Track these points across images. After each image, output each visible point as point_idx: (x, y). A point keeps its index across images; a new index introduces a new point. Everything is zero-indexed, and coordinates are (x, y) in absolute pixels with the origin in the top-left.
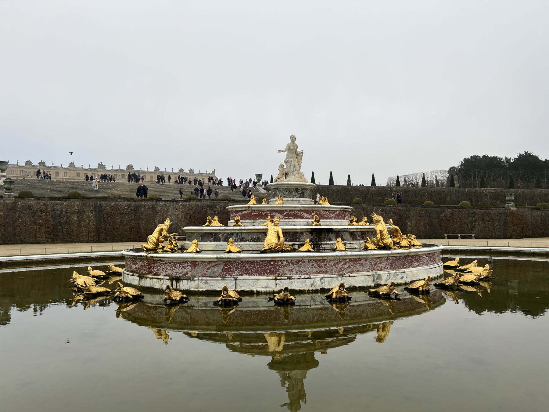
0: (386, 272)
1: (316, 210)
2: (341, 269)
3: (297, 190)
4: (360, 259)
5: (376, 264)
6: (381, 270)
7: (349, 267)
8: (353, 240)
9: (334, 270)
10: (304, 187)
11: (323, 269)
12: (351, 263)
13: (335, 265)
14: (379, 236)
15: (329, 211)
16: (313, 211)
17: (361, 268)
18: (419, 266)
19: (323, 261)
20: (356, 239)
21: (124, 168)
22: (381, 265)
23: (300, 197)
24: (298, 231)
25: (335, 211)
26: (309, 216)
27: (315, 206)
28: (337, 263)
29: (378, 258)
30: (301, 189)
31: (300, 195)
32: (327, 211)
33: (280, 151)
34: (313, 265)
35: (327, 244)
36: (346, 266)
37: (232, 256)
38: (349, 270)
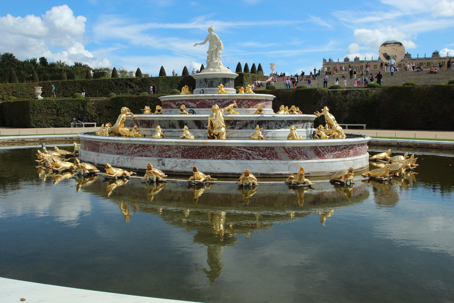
0: (173, 160)
1: (200, 100)
2: (132, 152)
3: (206, 80)
4: (147, 146)
5: (164, 151)
6: (170, 157)
7: (139, 151)
8: (199, 128)
9: (127, 153)
10: (210, 77)
11: (121, 151)
12: (140, 148)
13: (128, 148)
14: (209, 125)
15: (215, 100)
16: (198, 100)
17: (149, 154)
18: (227, 158)
19: (121, 144)
20: (203, 128)
21: (429, 55)
22: (169, 153)
23: (209, 87)
24: (150, 119)
25: (224, 100)
26: (194, 106)
27: (237, 94)
28: (130, 147)
29: (167, 146)
30: (210, 79)
31: (209, 84)
32: (213, 100)
33: (196, 44)
34: (115, 147)
35: (170, 131)
36: (136, 151)
38: (139, 154)
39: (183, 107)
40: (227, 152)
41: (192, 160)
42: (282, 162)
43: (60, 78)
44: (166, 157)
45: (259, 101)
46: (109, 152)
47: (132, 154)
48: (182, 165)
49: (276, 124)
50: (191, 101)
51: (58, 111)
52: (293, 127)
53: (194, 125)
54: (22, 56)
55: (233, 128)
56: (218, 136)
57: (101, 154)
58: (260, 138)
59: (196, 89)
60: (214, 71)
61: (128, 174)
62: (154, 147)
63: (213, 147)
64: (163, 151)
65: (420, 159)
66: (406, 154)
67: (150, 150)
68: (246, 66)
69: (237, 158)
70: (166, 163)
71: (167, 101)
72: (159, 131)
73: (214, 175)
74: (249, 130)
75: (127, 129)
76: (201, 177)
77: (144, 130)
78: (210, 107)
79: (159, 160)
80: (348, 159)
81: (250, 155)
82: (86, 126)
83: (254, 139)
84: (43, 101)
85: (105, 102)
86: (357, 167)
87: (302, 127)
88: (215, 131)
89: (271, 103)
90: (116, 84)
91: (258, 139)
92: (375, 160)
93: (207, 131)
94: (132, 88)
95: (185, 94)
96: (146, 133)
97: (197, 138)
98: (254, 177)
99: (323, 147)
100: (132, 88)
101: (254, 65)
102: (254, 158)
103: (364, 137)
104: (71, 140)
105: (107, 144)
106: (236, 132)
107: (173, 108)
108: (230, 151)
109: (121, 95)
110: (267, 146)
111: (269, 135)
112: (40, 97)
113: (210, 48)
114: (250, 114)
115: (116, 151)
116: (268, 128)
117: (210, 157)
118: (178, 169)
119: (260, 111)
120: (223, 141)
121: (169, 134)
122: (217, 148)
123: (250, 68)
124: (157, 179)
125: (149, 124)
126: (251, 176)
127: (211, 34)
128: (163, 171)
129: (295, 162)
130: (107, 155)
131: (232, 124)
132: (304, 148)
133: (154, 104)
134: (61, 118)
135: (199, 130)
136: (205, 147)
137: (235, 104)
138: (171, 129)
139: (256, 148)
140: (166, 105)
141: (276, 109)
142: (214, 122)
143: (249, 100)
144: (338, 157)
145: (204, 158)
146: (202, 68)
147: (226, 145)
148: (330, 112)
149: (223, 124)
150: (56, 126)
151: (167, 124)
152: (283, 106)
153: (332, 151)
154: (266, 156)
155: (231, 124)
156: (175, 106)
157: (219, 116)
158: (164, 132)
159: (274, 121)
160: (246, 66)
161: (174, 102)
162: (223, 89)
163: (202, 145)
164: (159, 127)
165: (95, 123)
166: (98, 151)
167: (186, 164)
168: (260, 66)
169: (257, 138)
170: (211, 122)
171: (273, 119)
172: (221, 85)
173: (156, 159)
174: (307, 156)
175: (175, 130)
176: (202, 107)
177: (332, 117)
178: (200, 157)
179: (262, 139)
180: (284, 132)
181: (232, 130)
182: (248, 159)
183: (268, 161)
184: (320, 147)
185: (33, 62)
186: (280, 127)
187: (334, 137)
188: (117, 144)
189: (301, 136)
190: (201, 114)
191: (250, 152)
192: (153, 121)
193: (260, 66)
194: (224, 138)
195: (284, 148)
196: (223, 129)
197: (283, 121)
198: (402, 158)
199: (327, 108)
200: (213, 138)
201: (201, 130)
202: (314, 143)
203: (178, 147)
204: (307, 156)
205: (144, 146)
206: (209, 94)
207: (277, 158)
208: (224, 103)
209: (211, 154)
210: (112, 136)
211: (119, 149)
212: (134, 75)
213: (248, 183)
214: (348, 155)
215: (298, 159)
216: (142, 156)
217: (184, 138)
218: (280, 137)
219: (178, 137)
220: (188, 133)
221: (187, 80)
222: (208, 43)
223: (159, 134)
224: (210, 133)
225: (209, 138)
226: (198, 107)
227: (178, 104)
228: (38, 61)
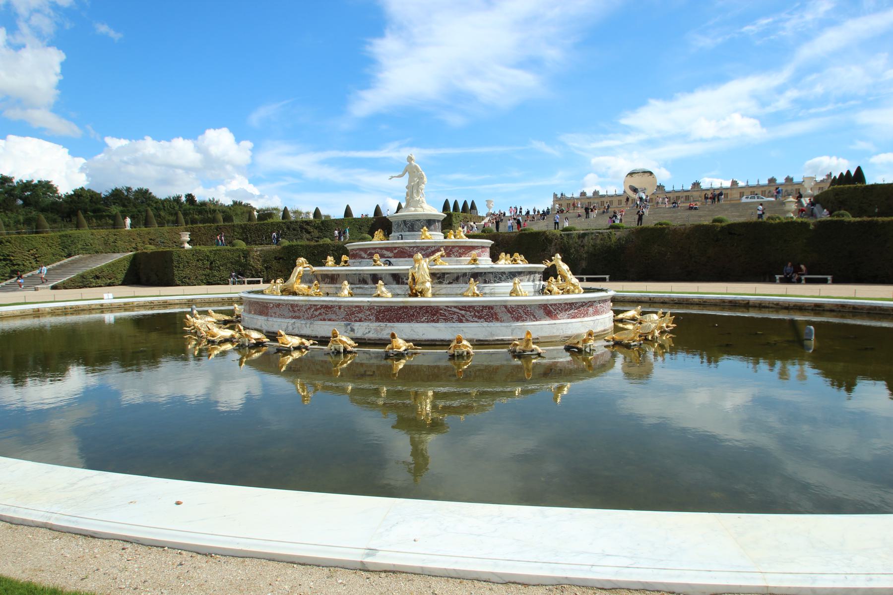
0: (365, 324)
3: (405, 221)
4: (332, 307)
6: (360, 321)
7: (320, 314)
8: (398, 283)
11: (297, 314)
12: (323, 310)
16: (395, 248)
18: (433, 321)
19: (297, 306)
20: (403, 283)
22: (360, 315)
26: (391, 255)
29: (357, 306)
37: (311, 298)
38: (320, 317)
39: (376, 257)
40: (433, 314)
41: (389, 324)
42: (503, 324)
43: (214, 220)
44: (356, 321)
45: (473, 248)
46: (282, 316)
47: (312, 317)
48: (376, 330)
49: (496, 277)
50: (387, 249)
51: (211, 263)
52: (517, 280)
53: (391, 279)
54: (161, 193)
55: (440, 283)
56: (422, 293)
57: (270, 319)
58: (475, 295)
59: (393, 234)
60: (415, 211)
61: (307, 343)
62: (340, 308)
63: (416, 307)
64: (352, 314)
65: (677, 318)
66: (661, 311)
67: (335, 313)
68: (456, 203)
69: (446, 320)
70: (355, 328)
71: (355, 250)
72: (346, 288)
73: (418, 343)
74: (461, 285)
75: (304, 286)
76: (401, 345)
77: (326, 287)
78: (411, 256)
79: (347, 325)
80: (586, 319)
81: (463, 316)
82: (250, 283)
83: (468, 296)
84: (191, 250)
85: (274, 251)
86: (598, 329)
87: (529, 281)
88: (418, 287)
89: (488, 250)
90: (288, 228)
91: (473, 296)
92: (621, 321)
93: (408, 286)
94: (309, 233)
95: (378, 240)
96: (330, 291)
97: (395, 295)
98: (468, 344)
99: (555, 305)
100: (309, 233)
101: (465, 203)
102: (467, 321)
103: (606, 291)
104: (230, 301)
105: (278, 305)
106: (445, 288)
107: (363, 258)
108: (437, 312)
109: (295, 243)
110: (485, 304)
111: (487, 290)
112: (187, 246)
113: (410, 182)
114: (463, 264)
115: (291, 314)
116: (485, 282)
117: (412, 320)
118: (372, 335)
119: (475, 260)
120: (429, 299)
121: (359, 291)
122: (421, 308)
123: (461, 206)
124: (345, 349)
125: (333, 279)
126: (465, 342)
127: (411, 164)
128: (352, 339)
129: (520, 324)
130: (279, 320)
131: (439, 278)
132: (530, 306)
133: (339, 253)
134: (215, 273)
135: (397, 286)
136: (406, 307)
137: (443, 252)
138: (362, 286)
139: (470, 307)
140: (355, 255)
141: (495, 258)
142: (416, 275)
143: (460, 247)
144: (574, 317)
145: (404, 322)
146: (399, 207)
147: (432, 305)
148: (563, 260)
149: (429, 278)
150: (209, 284)
151: (356, 279)
152: (503, 254)
153: (566, 310)
154: (483, 317)
155: (438, 277)
156: (366, 256)
157: (423, 267)
158: (352, 289)
159: (492, 273)
160: (456, 203)
161: (365, 250)
162: (427, 233)
163: (402, 305)
164: (346, 282)
165: (261, 279)
166: (267, 315)
167: (382, 330)
168: (473, 203)
169: (473, 295)
170: (413, 276)
171: (491, 271)
172: (425, 228)
173: (343, 323)
174: (534, 317)
175: (366, 286)
176: (401, 257)
177: (564, 267)
178: (399, 319)
179: (478, 296)
180: (505, 287)
181: (439, 286)
182: (461, 321)
183: (485, 324)
184: (551, 305)
185: (177, 200)
186: (500, 280)
187: (568, 292)
188: (292, 306)
189: (527, 291)
190: (400, 266)
191: (463, 312)
192: (339, 275)
193: (473, 203)
194: (430, 295)
195: (506, 307)
196: (428, 285)
197: (504, 273)
198: (655, 317)
199: (558, 256)
200: (416, 296)
201: (400, 286)
202: (542, 300)
203: (371, 308)
204: (534, 317)
205: (327, 307)
206: (410, 240)
207: (497, 320)
208: (429, 251)
209: (413, 315)
210: (286, 295)
211: (295, 311)
212: (311, 217)
213: (460, 352)
214: (586, 315)
215: (523, 321)
216: (324, 320)
217: (378, 296)
218: (500, 293)
219: (371, 295)
220: (384, 289)
221: (380, 223)
222: (407, 175)
223: (346, 292)
224: (411, 290)
225: (410, 296)
226: (395, 257)
227: (370, 253)
228: (183, 199)
